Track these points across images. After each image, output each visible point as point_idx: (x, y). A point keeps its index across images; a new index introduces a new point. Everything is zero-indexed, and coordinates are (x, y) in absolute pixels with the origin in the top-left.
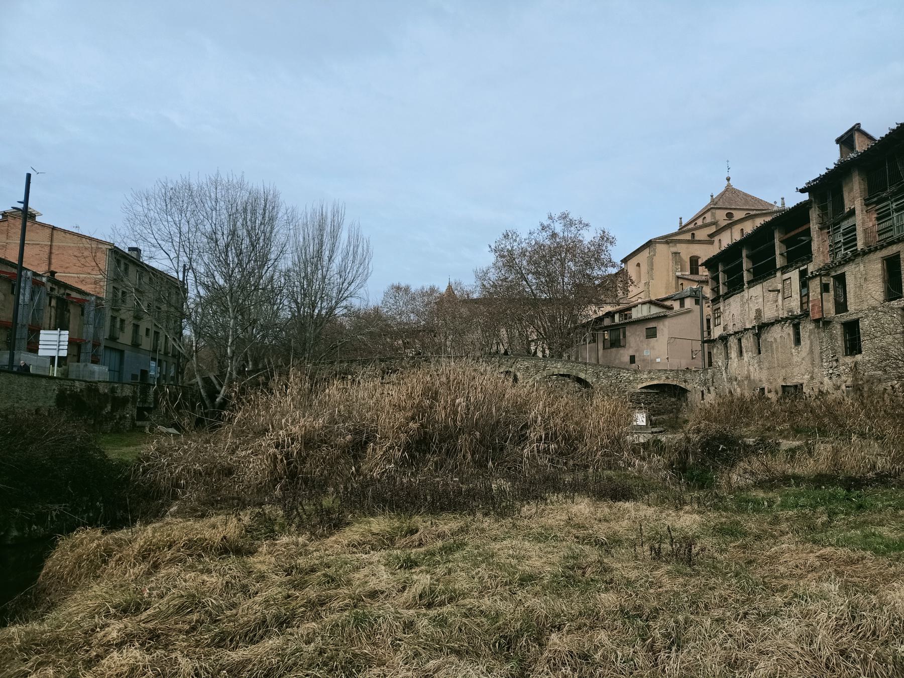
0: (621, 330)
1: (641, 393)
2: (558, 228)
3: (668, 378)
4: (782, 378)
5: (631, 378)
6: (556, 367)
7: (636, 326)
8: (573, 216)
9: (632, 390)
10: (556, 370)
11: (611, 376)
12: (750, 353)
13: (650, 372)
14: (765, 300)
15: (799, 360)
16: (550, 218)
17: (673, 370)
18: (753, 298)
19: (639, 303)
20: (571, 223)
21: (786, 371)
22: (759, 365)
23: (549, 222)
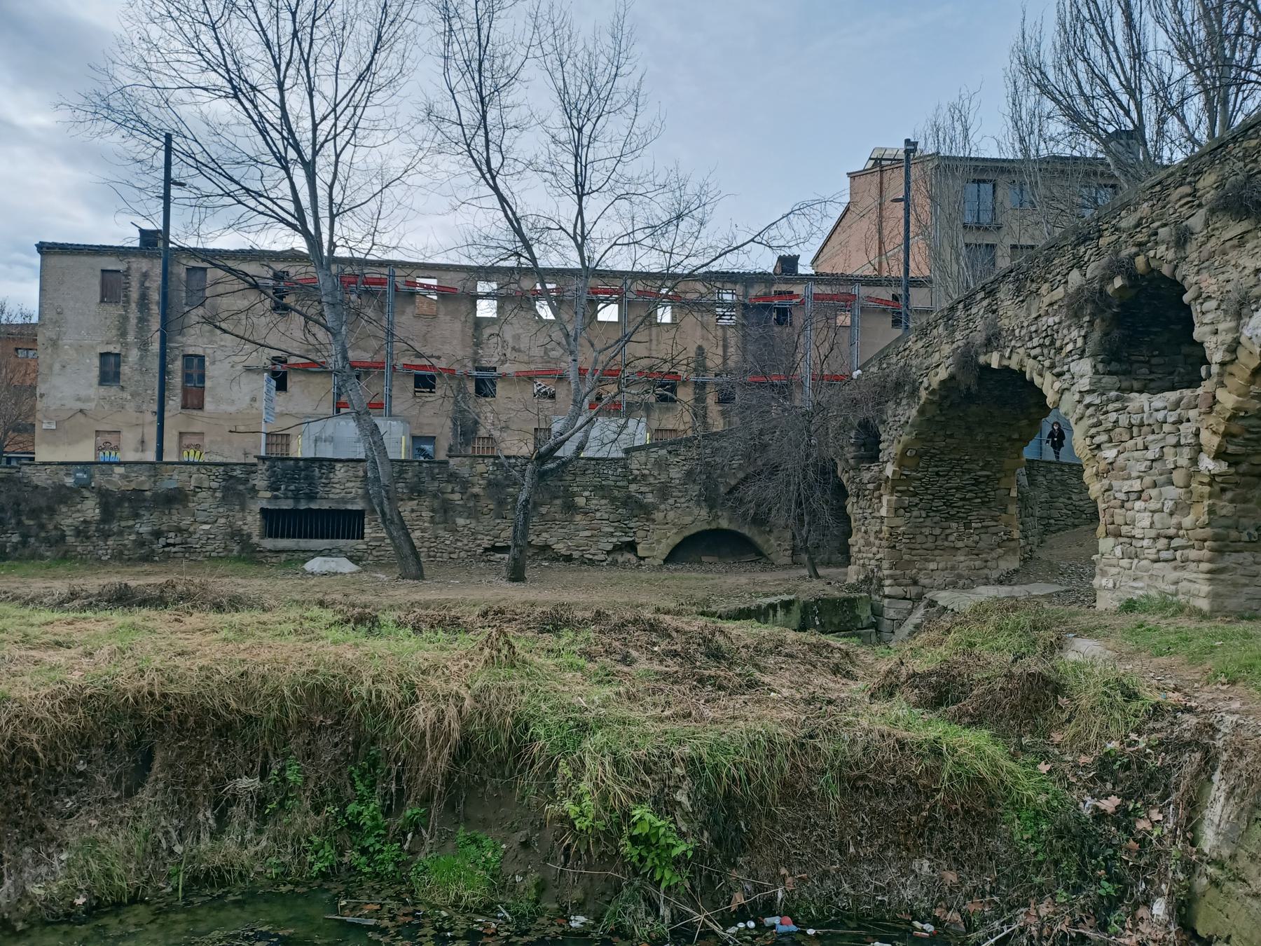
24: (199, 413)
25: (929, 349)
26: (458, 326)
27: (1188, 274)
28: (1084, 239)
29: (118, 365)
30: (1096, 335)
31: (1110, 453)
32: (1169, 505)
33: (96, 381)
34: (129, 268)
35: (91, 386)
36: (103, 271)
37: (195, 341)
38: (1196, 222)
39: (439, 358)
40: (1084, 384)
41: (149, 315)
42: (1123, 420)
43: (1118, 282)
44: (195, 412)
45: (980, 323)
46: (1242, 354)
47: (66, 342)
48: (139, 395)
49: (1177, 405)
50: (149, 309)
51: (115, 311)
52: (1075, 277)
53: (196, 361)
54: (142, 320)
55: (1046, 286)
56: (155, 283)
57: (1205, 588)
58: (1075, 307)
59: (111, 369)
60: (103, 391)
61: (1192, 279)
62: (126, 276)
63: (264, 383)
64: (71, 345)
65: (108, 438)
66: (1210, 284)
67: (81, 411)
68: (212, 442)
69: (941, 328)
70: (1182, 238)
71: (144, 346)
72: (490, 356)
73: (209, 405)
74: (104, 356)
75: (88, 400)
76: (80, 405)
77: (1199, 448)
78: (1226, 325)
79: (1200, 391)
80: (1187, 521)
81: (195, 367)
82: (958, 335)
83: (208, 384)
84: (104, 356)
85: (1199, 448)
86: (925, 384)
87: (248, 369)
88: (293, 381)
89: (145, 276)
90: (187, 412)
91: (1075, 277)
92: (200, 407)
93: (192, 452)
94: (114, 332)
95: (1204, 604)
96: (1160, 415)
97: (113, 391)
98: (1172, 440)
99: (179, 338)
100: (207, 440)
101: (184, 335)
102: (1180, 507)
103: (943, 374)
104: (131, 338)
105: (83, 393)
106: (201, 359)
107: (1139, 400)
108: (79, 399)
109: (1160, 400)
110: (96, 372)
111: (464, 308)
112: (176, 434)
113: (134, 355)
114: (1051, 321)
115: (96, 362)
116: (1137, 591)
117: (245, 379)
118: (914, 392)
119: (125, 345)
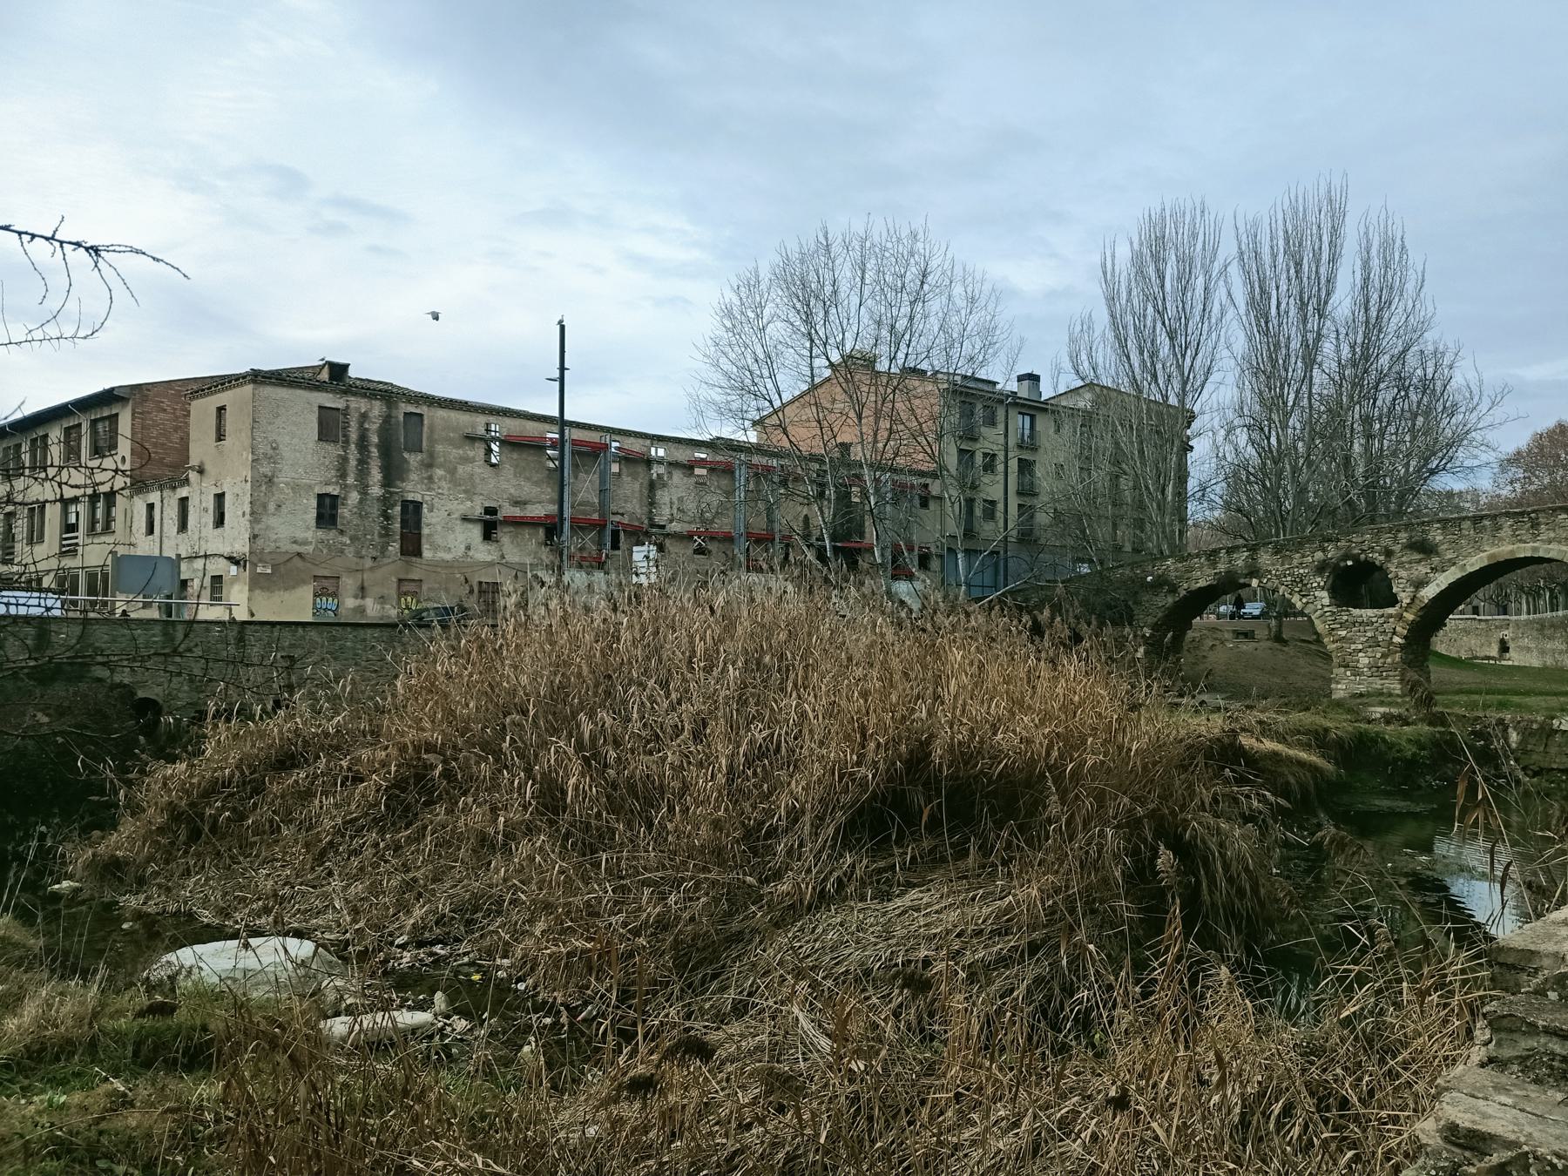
24: (418, 560)
25: (1190, 570)
26: (637, 486)
28: (1329, 540)
29: (334, 507)
30: (1330, 581)
31: (1343, 633)
32: (1379, 655)
33: (313, 523)
34: (348, 407)
35: (308, 528)
36: (320, 407)
37: (413, 489)
38: (1397, 548)
39: (622, 515)
40: (1326, 601)
41: (369, 457)
42: (1351, 619)
43: (1350, 563)
44: (414, 559)
45: (1240, 563)
46: (1417, 601)
47: (281, 480)
48: (358, 539)
49: (1382, 616)
50: (369, 452)
51: (334, 450)
52: (1319, 555)
53: (411, 507)
54: (363, 462)
56: (373, 426)
57: (1399, 686)
58: (1321, 568)
59: (327, 511)
60: (320, 533)
61: (1393, 569)
62: (345, 415)
63: (476, 532)
64: (287, 484)
65: (326, 583)
66: (1403, 573)
67: (299, 554)
68: (430, 589)
70: (1389, 553)
71: (364, 491)
72: (662, 516)
73: (427, 554)
74: (321, 497)
75: (305, 543)
76: (297, 548)
77: (1394, 633)
78: (1412, 589)
79: (1391, 611)
80: (1389, 660)
81: (413, 511)
83: (425, 531)
84: (321, 497)
85: (1394, 633)
87: (465, 519)
88: (505, 536)
89: (364, 417)
90: (408, 558)
91: (1319, 555)
92: (418, 553)
93: (409, 599)
94: (333, 473)
95: (1399, 692)
96: (1374, 620)
97: (333, 533)
98: (1381, 629)
99: (398, 483)
100: (425, 587)
101: (403, 481)
102: (1384, 656)
103: (1202, 583)
104: (350, 480)
105: (300, 535)
106: (418, 506)
107: (1356, 612)
108: (295, 542)
109: (1370, 612)
110: (313, 514)
111: (641, 469)
112: (394, 580)
113: (354, 497)
114: (1301, 571)
115: (314, 503)
116: (1362, 689)
117: (459, 527)
118: (1173, 589)
119: (345, 487)
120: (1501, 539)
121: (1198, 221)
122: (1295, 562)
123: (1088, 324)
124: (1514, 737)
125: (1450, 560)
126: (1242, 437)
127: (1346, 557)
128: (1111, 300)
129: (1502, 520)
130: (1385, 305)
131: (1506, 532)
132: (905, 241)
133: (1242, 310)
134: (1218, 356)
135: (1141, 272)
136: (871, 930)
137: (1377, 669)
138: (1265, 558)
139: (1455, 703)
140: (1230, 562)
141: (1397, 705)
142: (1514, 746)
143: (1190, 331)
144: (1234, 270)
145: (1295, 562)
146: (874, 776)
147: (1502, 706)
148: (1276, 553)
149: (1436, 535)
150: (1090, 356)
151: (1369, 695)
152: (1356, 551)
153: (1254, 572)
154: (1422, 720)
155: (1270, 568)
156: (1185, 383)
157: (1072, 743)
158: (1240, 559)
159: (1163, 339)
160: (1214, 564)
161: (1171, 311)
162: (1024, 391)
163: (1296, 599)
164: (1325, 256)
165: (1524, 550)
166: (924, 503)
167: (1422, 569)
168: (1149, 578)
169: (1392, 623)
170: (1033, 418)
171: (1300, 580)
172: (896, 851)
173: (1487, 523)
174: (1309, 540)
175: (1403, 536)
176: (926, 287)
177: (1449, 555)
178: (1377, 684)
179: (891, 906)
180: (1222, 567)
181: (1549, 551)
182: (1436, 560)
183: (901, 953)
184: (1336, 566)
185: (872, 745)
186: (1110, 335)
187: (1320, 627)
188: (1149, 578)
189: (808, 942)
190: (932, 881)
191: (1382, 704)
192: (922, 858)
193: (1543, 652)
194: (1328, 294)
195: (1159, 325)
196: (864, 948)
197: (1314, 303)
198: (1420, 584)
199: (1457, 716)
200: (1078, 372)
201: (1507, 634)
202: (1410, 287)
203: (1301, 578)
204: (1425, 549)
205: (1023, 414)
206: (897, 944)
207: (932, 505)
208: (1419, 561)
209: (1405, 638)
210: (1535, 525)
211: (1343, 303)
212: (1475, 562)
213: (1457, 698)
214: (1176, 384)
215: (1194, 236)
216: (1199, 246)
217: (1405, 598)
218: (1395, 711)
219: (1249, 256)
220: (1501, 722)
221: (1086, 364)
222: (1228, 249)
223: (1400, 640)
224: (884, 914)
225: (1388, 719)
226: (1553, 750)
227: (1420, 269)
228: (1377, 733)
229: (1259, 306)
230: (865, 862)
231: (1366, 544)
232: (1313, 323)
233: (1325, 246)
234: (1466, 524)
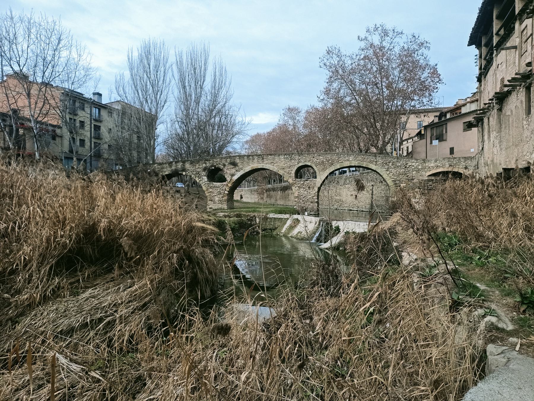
0: (444, 126)
1: (429, 180)
2: (376, 40)
3: (450, 166)
4: (515, 159)
5: (420, 167)
6: (348, 160)
7: (455, 121)
8: (389, 26)
9: (421, 178)
10: (348, 162)
11: (400, 166)
12: (495, 133)
13: (436, 161)
14: (508, 65)
15: (529, 134)
16: (368, 31)
17: (456, 158)
18: (500, 66)
19: (468, 102)
20: (385, 33)
21: (518, 150)
22: (500, 146)
23: (367, 35)
25: (163, 168)
27: (225, 170)
31: (211, 190)
38: (227, 164)
40: (206, 180)
42: (213, 186)
43: (213, 168)
45: (179, 167)
55: (198, 165)
58: (204, 169)
66: (228, 172)
69: (167, 165)
70: (224, 165)
79: (224, 183)
80: (224, 199)
82: (173, 167)
86: (161, 174)
91: (204, 165)
102: (223, 197)
107: (215, 183)
116: (216, 208)
120: (254, 162)
121: (162, 47)
122: (197, 167)
123: (122, 76)
124: (258, 220)
125: (241, 168)
126: (177, 126)
127: (212, 166)
128: (131, 69)
129: (255, 157)
130: (220, 88)
131: (256, 160)
132: (50, 24)
133: (177, 82)
134: (168, 96)
135: (141, 61)
136: (72, 309)
137: (220, 201)
138: (187, 165)
139: (242, 211)
140: (176, 166)
141: (226, 212)
142: (258, 223)
143: (159, 86)
144: (175, 67)
145: (197, 167)
146: (70, 241)
147: (254, 211)
148: (191, 164)
149: (237, 160)
150: (123, 89)
151: (218, 209)
152: (215, 164)
153: (184, 170)
154: (234, 216)
155: (189, 169)
156: (157, 104)
157: (155, 223)
158: (180, 165)
159: (149, 86)
160: (171, 167)
161: (152, 77)
162: (96, 98)
163: (197, 179)
164: (203, 68)
165: (260, 166)
166: (54, 138)
167: (233, 171)
168: (149, 170)
169: (225, 187)
170: (99, 110)
171: (198, 173)
172: (80, 274)
173: (251, 157)
174: (201, 160)
175: (228, 160)
176: (60, 46)
177: (241, 167)
178: (220, 206)
179: (80, 297)
180: (173, 168)
181: (266, 166)
182: (237, 168)
183: (89, 317)
184: (209, 169)
185: (68, 228)
186: (131, 82)
187: (204, 188)
188: (149, 170)
189: (39, 320)
190: (97, 284)
191: (222, 212)
192: (92, 275)
193: (251, 198)
194: (204, 82)
195: (148, 82)
196: (70, 318)
197: (199, 84)
198: (233, 175)
199: (243, 214)
200: (119, 95)
201: (243, 193)
202: (227, 83)
203: (199, 172)
204: (234, 164)
205: (96, 108)
206: (87, 314)
207: (57, 139)
208: (233, 168)
209: (228, 192)
210: (263, 159)
211: (208, 86)
212: (248, 169)
213: (242, 209)
214: (155, 104)
215: (161, 52)
216: (162, 56)
217: (228, 179)
218: (226, 214)
219: (180, 64)
220: (254, 216)
221: (122, 91)
222: (172, 59)
223: (228, 193)
224: (77, 302)
225: (225, 216)
226: (268, 223)
227: (230, 79)
228: (224, 220)
229: (182, 80)
230: (65, 280)
231: (217, 162)
232: (199, 90)
233: (203, 65)
234: (246, 157)
